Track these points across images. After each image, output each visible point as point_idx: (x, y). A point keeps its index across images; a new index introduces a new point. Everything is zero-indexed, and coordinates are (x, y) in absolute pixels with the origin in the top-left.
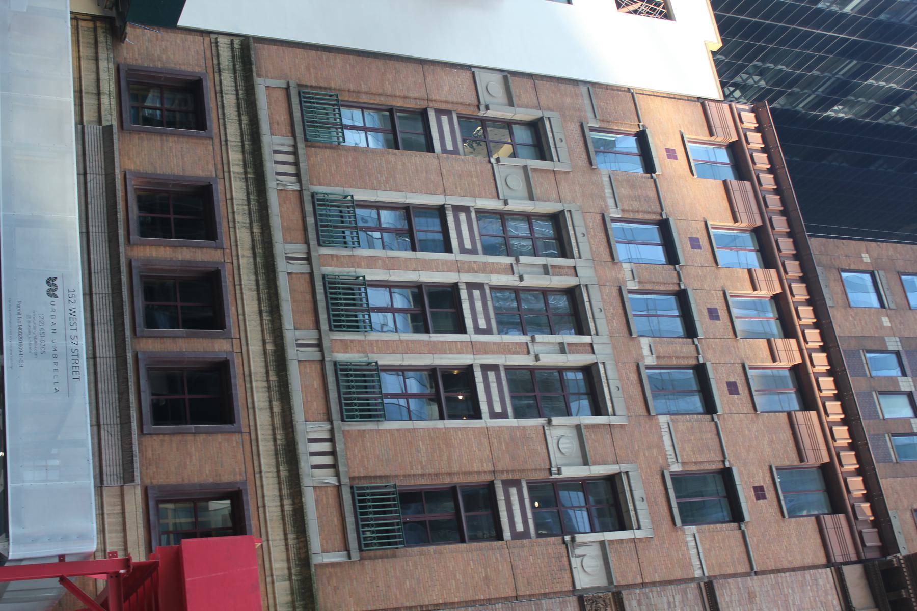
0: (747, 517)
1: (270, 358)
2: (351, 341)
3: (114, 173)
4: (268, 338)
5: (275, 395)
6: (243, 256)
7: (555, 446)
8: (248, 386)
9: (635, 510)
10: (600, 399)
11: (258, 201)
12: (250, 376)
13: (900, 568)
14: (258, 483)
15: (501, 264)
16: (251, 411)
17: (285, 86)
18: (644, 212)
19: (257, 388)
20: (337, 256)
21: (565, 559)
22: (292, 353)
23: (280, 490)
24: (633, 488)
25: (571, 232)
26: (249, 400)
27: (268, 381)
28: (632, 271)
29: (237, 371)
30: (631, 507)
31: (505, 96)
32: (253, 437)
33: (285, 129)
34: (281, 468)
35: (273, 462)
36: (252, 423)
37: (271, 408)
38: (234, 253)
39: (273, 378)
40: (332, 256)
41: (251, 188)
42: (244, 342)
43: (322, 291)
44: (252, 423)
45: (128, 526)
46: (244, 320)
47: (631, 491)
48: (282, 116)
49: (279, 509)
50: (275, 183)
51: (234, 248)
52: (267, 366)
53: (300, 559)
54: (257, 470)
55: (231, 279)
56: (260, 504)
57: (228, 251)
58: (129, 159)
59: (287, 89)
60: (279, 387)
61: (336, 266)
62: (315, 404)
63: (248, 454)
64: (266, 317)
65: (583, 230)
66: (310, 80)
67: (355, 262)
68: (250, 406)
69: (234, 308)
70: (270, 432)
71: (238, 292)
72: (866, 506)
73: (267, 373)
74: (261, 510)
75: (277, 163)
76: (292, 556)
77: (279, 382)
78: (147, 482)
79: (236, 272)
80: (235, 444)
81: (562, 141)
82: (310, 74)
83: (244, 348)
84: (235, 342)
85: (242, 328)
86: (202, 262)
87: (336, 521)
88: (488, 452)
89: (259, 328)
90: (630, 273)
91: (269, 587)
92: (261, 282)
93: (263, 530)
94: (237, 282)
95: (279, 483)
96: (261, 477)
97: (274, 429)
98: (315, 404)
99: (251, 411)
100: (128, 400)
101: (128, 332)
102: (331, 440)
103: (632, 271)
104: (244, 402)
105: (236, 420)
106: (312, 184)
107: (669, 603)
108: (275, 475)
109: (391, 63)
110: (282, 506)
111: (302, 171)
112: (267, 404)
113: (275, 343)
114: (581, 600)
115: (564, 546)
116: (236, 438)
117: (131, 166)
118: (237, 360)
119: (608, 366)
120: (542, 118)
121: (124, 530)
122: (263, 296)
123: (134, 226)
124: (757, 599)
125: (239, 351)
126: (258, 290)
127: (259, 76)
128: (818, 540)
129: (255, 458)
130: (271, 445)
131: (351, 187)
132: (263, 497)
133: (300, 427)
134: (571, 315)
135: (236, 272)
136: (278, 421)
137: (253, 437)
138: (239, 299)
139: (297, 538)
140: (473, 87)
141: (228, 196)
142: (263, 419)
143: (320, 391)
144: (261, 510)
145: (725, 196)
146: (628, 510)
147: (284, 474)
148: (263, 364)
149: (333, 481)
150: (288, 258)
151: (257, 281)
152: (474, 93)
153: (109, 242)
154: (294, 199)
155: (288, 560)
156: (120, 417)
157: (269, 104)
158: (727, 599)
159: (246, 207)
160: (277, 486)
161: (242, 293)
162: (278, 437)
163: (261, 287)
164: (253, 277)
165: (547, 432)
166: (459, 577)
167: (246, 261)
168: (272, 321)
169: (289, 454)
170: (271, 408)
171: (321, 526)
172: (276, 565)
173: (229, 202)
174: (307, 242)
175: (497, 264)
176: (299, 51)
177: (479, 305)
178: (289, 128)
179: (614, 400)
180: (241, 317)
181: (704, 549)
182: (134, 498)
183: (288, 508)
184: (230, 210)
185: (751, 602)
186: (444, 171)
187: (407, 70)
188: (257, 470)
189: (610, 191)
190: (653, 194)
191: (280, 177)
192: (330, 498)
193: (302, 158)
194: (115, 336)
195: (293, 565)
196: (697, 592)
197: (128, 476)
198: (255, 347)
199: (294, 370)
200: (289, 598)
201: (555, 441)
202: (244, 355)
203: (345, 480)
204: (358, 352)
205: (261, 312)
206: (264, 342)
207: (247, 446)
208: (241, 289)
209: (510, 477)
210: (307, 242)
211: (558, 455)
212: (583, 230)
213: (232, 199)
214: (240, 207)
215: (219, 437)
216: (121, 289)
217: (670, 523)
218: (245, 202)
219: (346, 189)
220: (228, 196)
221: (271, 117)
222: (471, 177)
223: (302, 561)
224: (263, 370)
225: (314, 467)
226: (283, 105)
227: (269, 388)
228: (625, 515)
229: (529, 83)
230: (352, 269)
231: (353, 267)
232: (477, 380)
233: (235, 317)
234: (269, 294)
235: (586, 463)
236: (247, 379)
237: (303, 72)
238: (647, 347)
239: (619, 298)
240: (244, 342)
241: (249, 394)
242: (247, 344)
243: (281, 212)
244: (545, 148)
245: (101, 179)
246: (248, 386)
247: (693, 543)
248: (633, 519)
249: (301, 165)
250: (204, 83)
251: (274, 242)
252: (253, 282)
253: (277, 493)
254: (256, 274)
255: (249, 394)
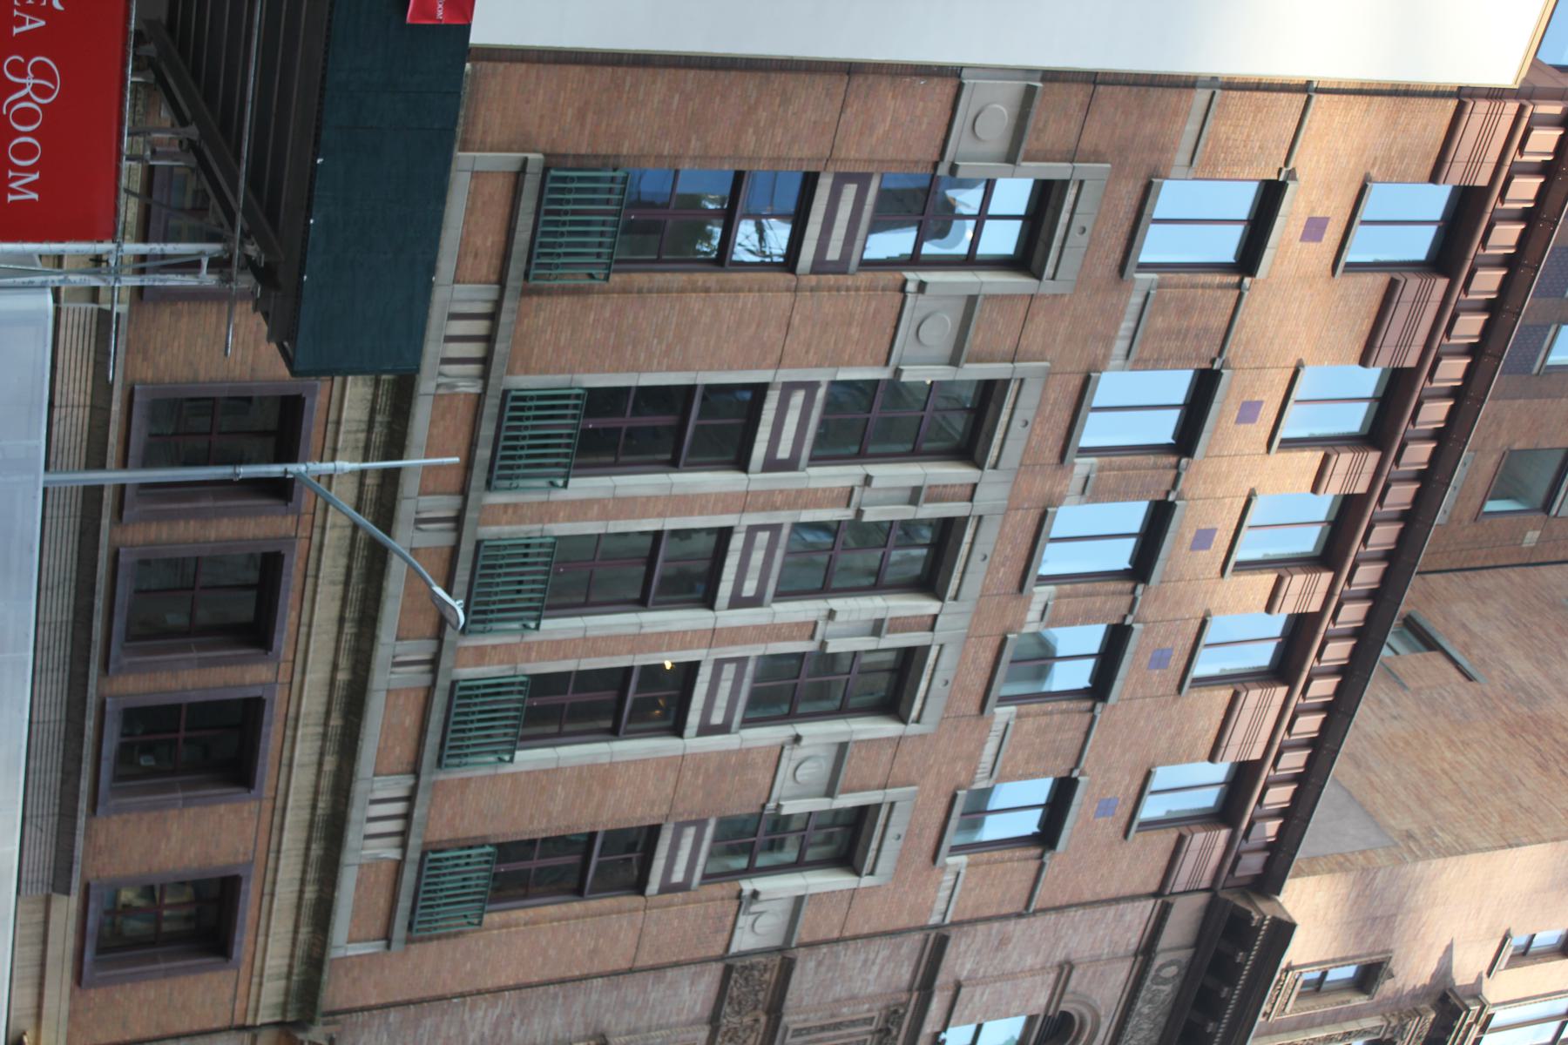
0: (1061, 845)
1: (339, 693)
2: (494, 647)
3: (109, 410)
4: (344, 662)
5: (331, 746)
6: (334, 526)
7: (790, 771)
8: (289, 733)
9: (879, 850)
10: (908, 686)
11: (389, 425)
12: (297, 719)
13: (1258, 929)
14: (271, 864)
15: (831, 490)
16: (284, 770)
17: (515, 168)
18: (1210, 286)
19: (334, 526)
20: (516, 506)
21: (731, 918)
22: (382, 678)
23: (304, 872)
24: (1078, 210)
25: (1004, 418)
26: (286, 754)
27: (326, 724)
28: (1087, 478)
29: (250, 895)
30: (874, 845)
31: (1009, 134)
32: (279, 803)
33: (487, 266)
34: (314, 846)
35: (303, 835)
36: (282, 785)
37: (320, 764)
38: (318, 521)
39: (336, 721)
40: (506, 506)
41: (382, 401)
42: (298, 669)
43: (467, 578)
44: (282, 785)
45: (45, 1012)
46: (309, 635)
47: (886, 826)
48: (489, 240)
49: (295, 896)
50: (433, 384)
51: (319, 514)
52: (329, 703)
53: (309, 956)
54: (273, 846)
55: (301, 565)
56: (267, 889)
57: (308, 518)
58: (145, 359)
59: (520, 174)
60: (343, 734)
61: (509, 523)
62: (398, 750)
63: (265, 825)
64: (349, 629)
65: (988, 550)
66: (578, 142)
67: (548, 512)
68: (285, 761)
69: (293, 615)
70: (310, 796)
71: (309, 587)
72: (1271, 828)
73: (328, 713)
74: (266, 899)
75: (450, 339)
76: (299, 952)
77: (344, 728)
78: (91, 875)
79: (313, 554)
80: (245, 815)
81: (1084, 230)
82: (583, 125)
83: (297, 678)
84: (285, 668)
85: (301, 646)
86: (255, 539)
87: (382, 903)
88: (669, 790)
89: (332, 645)
90: (1081, 482)
91: (254, 989)
92: (355, 573)
93: (263, 923)
94: (311, 572)
95: (306, 863)
96: (278, 859)
97: (316, 792)
98: (398, 750)
99: (284, 770)
100: (77, 787)
101: (83, 805)
102: (493, 317)
103: (1087, 478)
104: (277, 756)
105: (295, 497)
106: (510, 372)
107: (866, 961)
108: (302, 852)
109: (778, 79)
110: (301, 892)
111: (496, 359)
112: (315, 758)
113: (354, 670)
114: (728, 970)
115: (736, 903)
116: (254, 806)
117: (145, 372)
118: (280, 695)
119: (947, 651)
120: (1065, 184)
121: (45, 942)
122: (353, 595)
123: (119, 624)
124: (1010, 947)
125: (287, 680)
126: (347, 583)
127: (463, 149)
128: (1163, 862)
129: (275, 832)
130: (305, 815)
131: (589, 371)
132: (274, 883)
133: (360, 789)
134: (970, 410)
135: (313, 554)
136: (326, 783)
137: (279, 803)
138: (308, 597)
139: (314, 932)
140: (946, 119)
141: (333, 416)
142: (302, 780)
143: (413, 732)
144: (266, 899)
145: (1375, 309)
146: (959, 543)
147: (316, 850)
148: (324, 699)
149: (395, 854)
150: (419, 521)
151: (349, 569)
152: (941, 135)
153: (82, 534)
154: (464, 412)
155: (292, 956)
156: (61, 805)
157: (470, 211)
158: (963, 948)
159: (362, 436)
160: (299, 867)
161: (315, 592)
162: (321, 805)
163: (354, 580)
164: (343, 561)
165: (786, 753)
166: (552, 952)
167: (313, 701)
168: (358, 636)
169: (332, 830)
170: (320, 764)
171: (356, 912)
172: (269, 962)
173: (331, 427)
174: (502, 282)
175: (824, 490)
176: (576, 71)
177: (757, 557)
178: (496, 262)
179: (929, 700)
180: (303, 629)
181: (964, 889)
182: (66, 909)
183: (342, 676)
184: (329, 443)
185: (997, 949)
186: (796, 320)
187: (811, 100)
188: (273, 846)
189: (1132, 325)
190: (1220, 322)
191: (448, 369)
192: (499, 190)
193: (502, 333)
194: (69, 689)
195: (297, 963)
196: (919, 946)
197: (60, 880)
198: (317, 674)
199: (376, 706)
200: (281, 999)
201: (793, 765)
202: (295, 690)
203: (413, 854)
204: (501, 662)
205: (341, 620)
206: (335, 667)
207: (266, 817)
208: (316, 585)
209: (831, 279)
210: (502, 282)
211: (789, 783)
212: (988, 550)
213: (338, 423)
214: (351, 437)
215: (222, 808)
216: (90, 620)
217: (931, 854)
218: (364, 426)
219: (576, 377)
220: (333, 416)
221: (464, 242)
222: (850, 324)
223: (313, 964)
224: (322, 709)
225: (447, 361)
226: (499, 211)
227: (324, 736)
228: (1040, 246)
229: (1079, 94)
230: (539, 526)
231: (541, 521)
232: (699, 679)
233: (293, 629)
234: (365, 592)
235: (954, 361)
236: (291, 723)
237: (563, 121)
238: (1040, 607)
239: (1075, 396)
240: (298, 669)
241: (287, 745)
242: (304, 672)
243: (430, 436)
244: (1043, 234)
245: (82, 416)
246: (289, 733)
247: (943, 907)
248: (994, 452)
249: (500, 347)
250: (243, 887)
251: (399, 496)
252: (341, 570)
253: (298, 875)
254: (351, 556)
255: (287, 745)
